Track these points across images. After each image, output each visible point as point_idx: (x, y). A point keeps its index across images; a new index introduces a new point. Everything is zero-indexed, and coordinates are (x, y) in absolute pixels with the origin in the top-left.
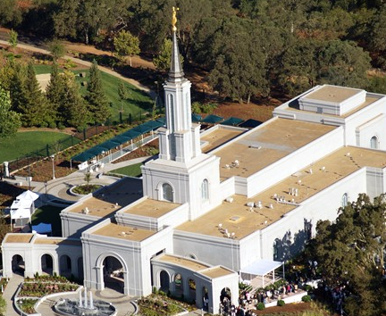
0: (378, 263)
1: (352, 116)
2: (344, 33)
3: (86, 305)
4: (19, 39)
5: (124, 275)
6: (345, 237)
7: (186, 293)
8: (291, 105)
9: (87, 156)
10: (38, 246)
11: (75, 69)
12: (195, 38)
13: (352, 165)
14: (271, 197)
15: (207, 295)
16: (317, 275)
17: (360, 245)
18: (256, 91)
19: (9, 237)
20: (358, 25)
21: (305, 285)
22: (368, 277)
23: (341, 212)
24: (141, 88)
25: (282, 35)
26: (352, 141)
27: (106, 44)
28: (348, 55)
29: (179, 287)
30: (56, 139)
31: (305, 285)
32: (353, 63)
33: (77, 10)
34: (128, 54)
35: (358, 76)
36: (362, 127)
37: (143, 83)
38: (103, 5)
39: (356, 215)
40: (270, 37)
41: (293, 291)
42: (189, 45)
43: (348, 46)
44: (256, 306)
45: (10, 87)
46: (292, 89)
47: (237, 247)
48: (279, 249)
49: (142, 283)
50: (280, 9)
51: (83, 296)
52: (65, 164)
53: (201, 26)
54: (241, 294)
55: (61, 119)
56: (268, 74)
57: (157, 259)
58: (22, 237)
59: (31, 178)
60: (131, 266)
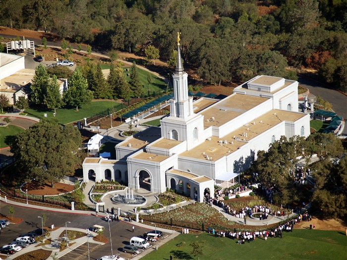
0: (292, 174)
1: (277, 93)
2: (272, 47)
3: (130, 197)
4: (93, 50)
5: (151, 181)
6: (273, 160)
7: (185, 191)
8: (243, 87)
9: (130, 115)
10: (103, 165)
11: (123, 67)
12: (190, 49)
13: (277, 120)
14: (232, 138)
15: (197, 192)
16: (258, 181)
17: (282, 164)
18: (224, 79)
19: (87, 160)
20: (280, 42)
21: (251, 186)
22: (286, 182)
23: (271, 146)
24: (160, 77)
25: (238, 48)
26: (277, 107)
27: (141, 53)
28: (275, 58)
29: (181, 188)
30: (113, 105)
31: (251, 186)
32: (277, 63)
33: (125, 34)
34: (153, 58)
35: (281, 71)
36: (283, 99)
37: (161, 74)
38: (139, 31)
39: (279, 148)
40: (232, 49)
41: (244, 190)
42: (187, 53)
43: (275, 54)
44: (224, 198)
45: (88, 76)
46: (244, 78)
47: (213, 165)
48: (237, 166)
49: (161, 186)
50: (237, 33)
51: (128, 192)
52: (118, 119)
53: (193, 43)
54: (215, 192)
55: (116, 94)
56: (230, 69)
57: (169, 172)
58: (94, 160)
59: (99, 127)
60: (154, 176)
